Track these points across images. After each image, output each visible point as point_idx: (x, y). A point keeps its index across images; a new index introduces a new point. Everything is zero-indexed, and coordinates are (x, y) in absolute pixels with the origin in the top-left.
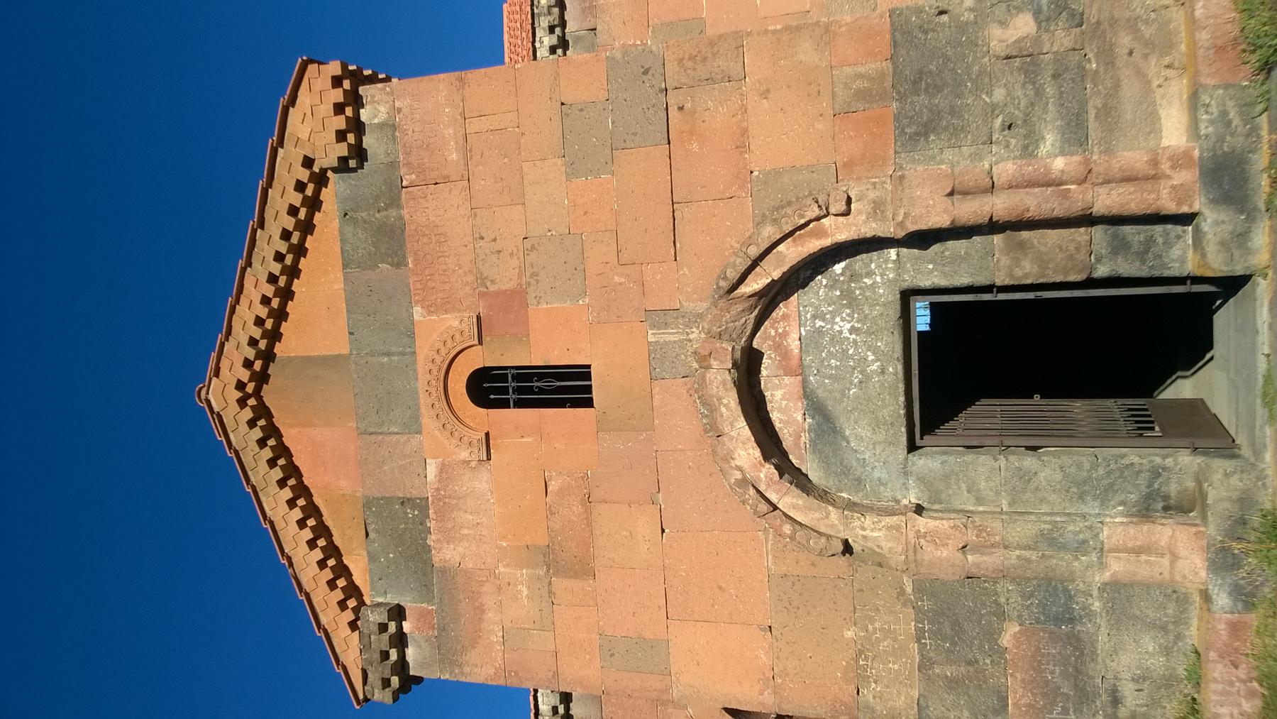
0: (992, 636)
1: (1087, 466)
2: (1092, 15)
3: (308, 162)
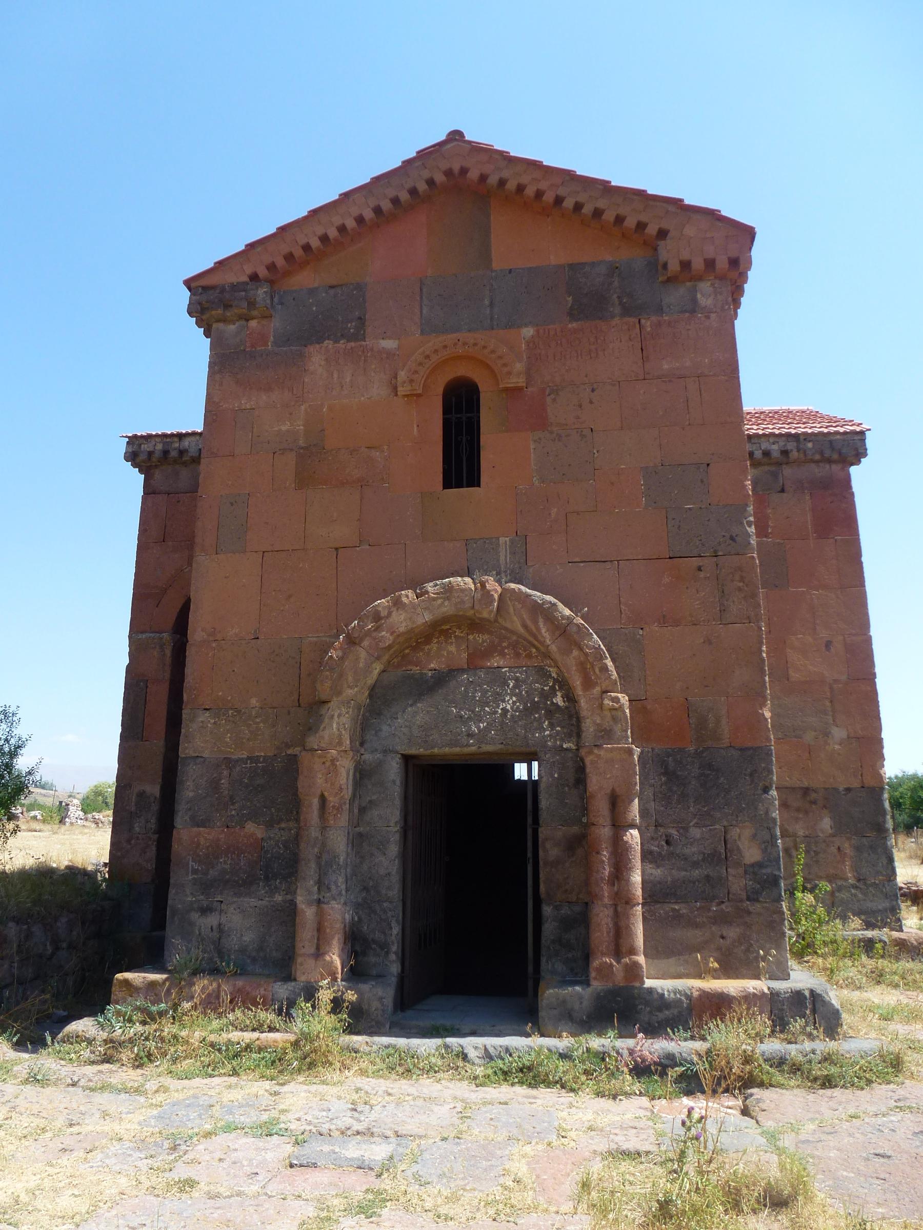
1: (390, 894)
3: (662, 234)
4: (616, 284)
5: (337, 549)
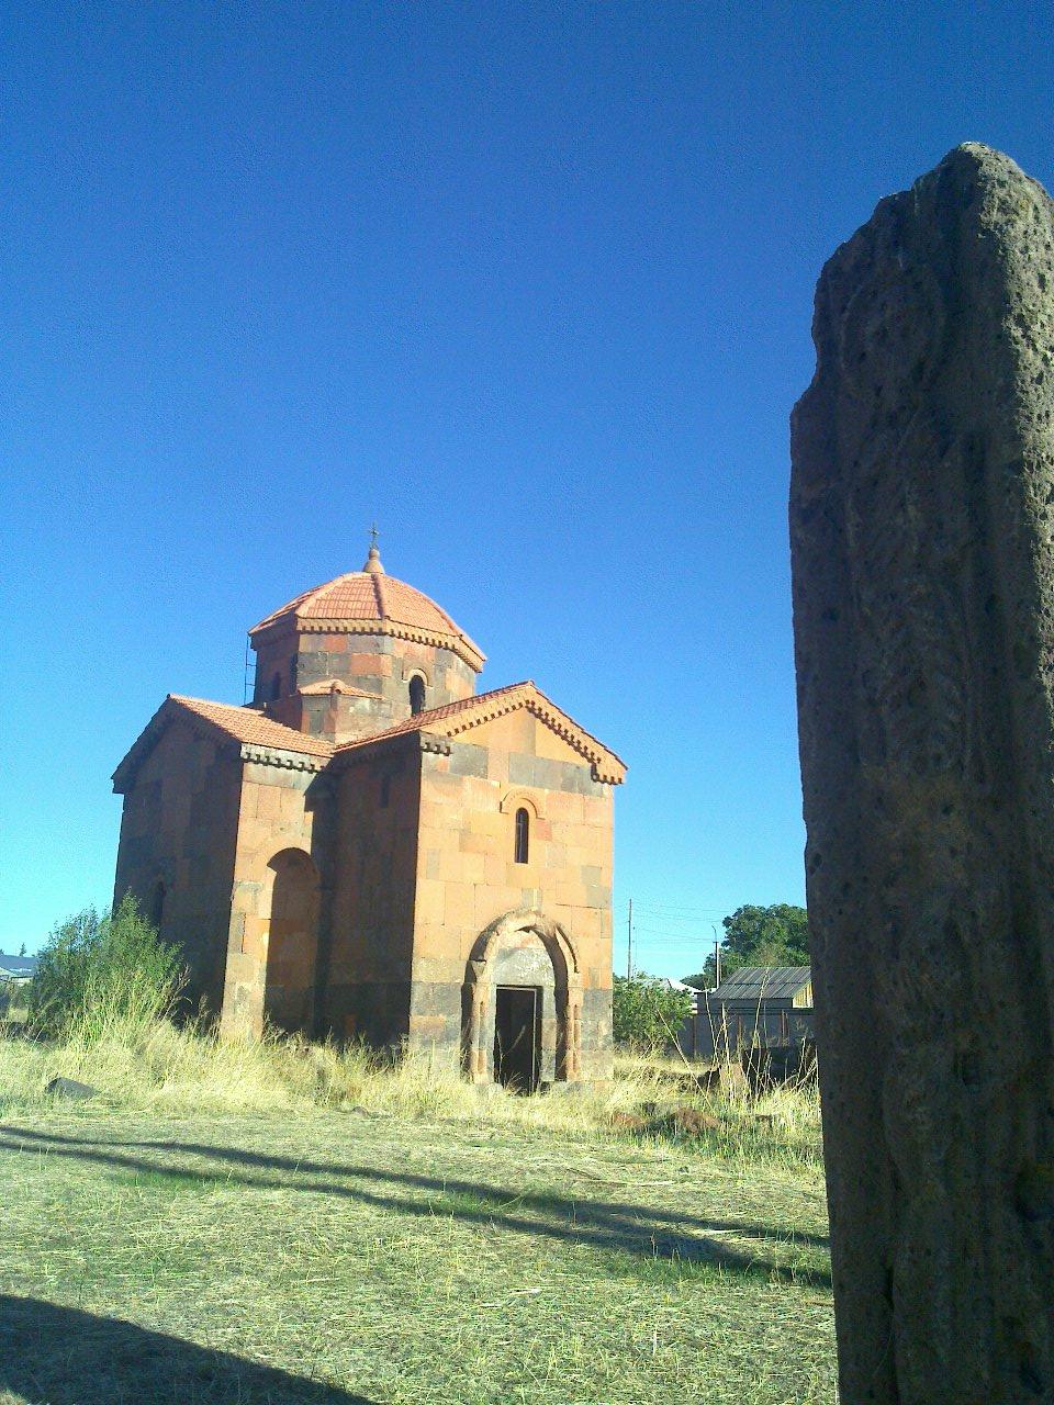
0: (442, 1011)
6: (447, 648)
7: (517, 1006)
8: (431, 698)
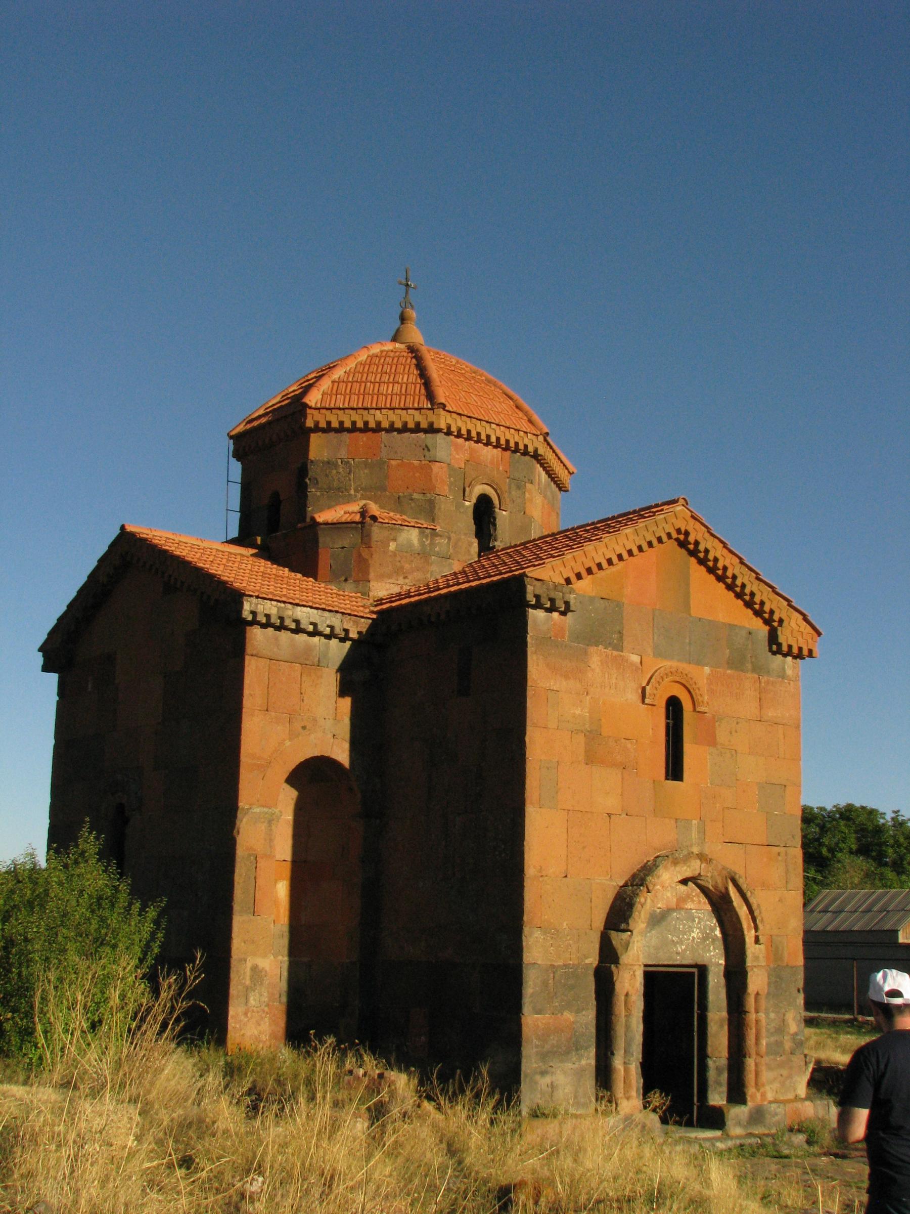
0: (568, 1006)
2: (794, 1058)
4: (750, 646)
5: (609, 815)
6: (525, 453)
7: (673, 994)
8: (506, 533)
